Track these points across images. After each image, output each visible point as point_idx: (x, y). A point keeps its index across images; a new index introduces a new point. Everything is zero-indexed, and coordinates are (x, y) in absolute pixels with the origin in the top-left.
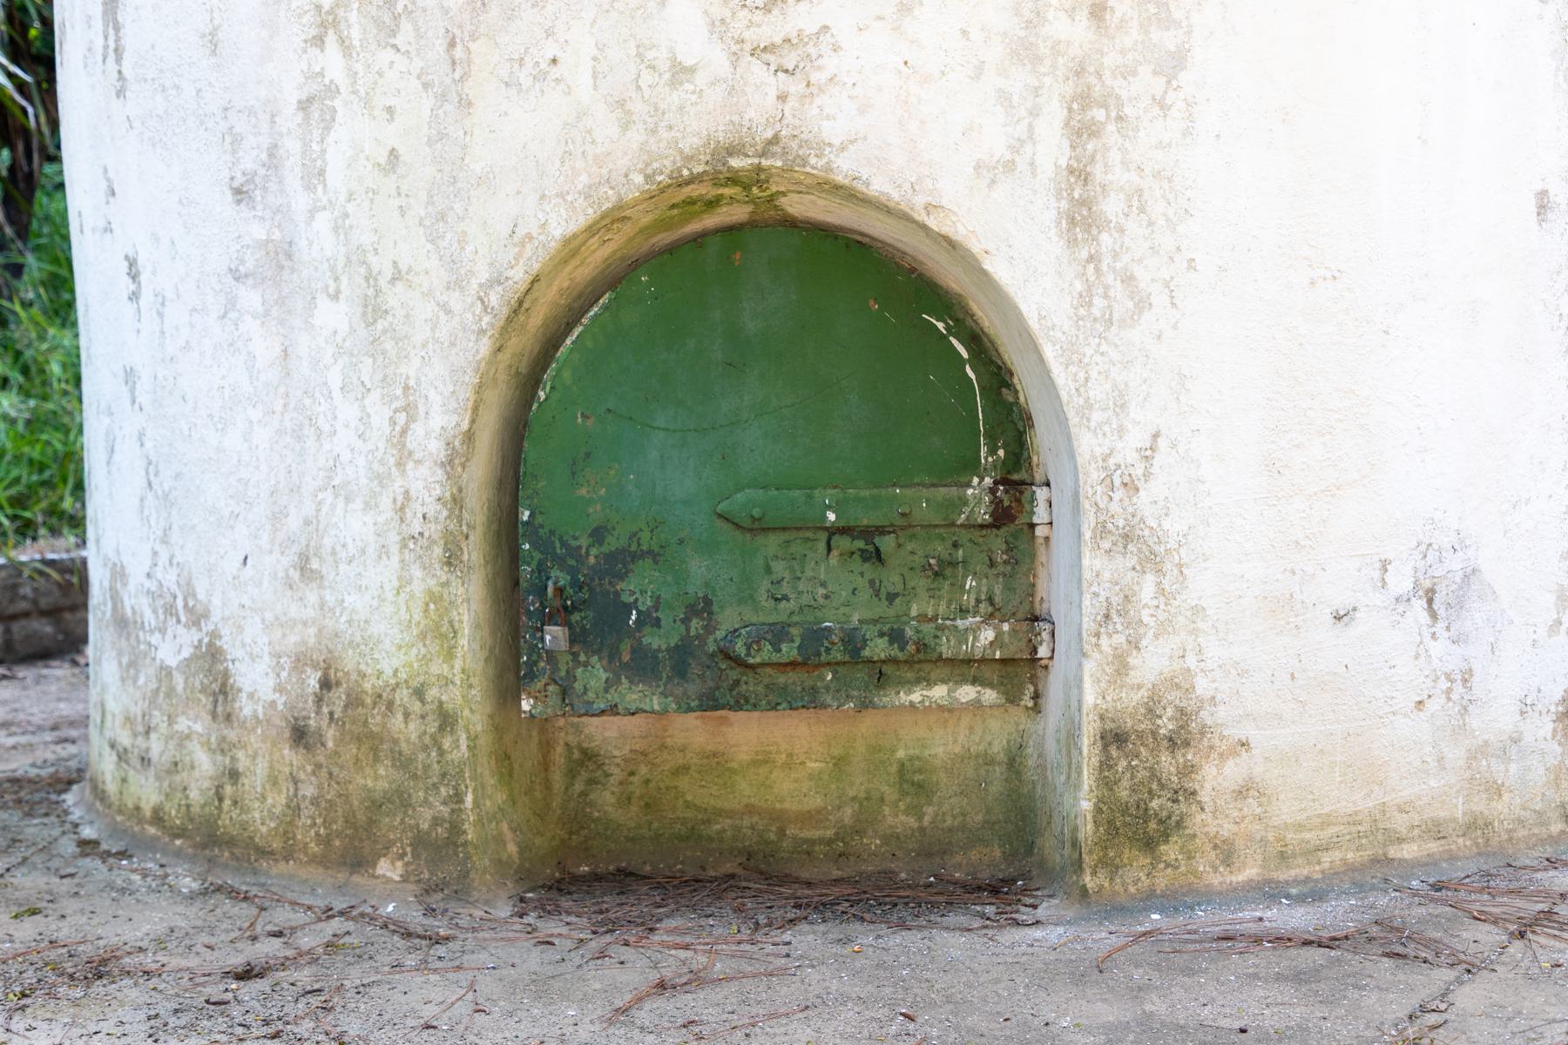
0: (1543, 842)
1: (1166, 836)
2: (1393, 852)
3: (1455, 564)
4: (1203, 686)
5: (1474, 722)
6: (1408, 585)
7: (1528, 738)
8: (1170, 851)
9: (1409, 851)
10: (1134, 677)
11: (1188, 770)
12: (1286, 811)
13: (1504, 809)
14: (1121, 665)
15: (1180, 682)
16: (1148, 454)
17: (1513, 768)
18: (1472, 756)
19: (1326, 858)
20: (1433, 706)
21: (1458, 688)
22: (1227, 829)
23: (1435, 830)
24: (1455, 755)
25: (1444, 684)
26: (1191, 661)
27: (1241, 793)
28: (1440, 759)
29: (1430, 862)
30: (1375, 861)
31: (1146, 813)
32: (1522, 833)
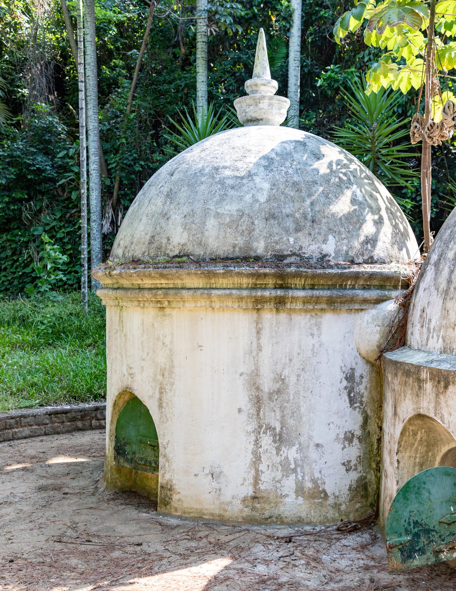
0: (236, 522)
1: (168, 504)
2: (203, 516)
3: (218, 470)
4: (174, 482)
5: (221, 498)
6: (208, 472)
7: (234, 503)
8: (168, 507)
9: (206, 517)
10: (165, 478)
11: (171, 495)
12: (185, 505)
13: (227, 515)
14: (163, 476)
15: (171, 480)
16: (168, 443)
17: (230, 507)
18: (221, 504)
19: (192, 515)
20: (213, 493)
21: (218, 492)
22: (176, 506)
23: (212, 515)
24: (217, 503)
25: (215, 490)
26: (173, 477)
27: (179, 500)
28: (214, 503)
29: (210, 520)
30: (200, 517)
31: (165, 500)
32: (231, 519)
